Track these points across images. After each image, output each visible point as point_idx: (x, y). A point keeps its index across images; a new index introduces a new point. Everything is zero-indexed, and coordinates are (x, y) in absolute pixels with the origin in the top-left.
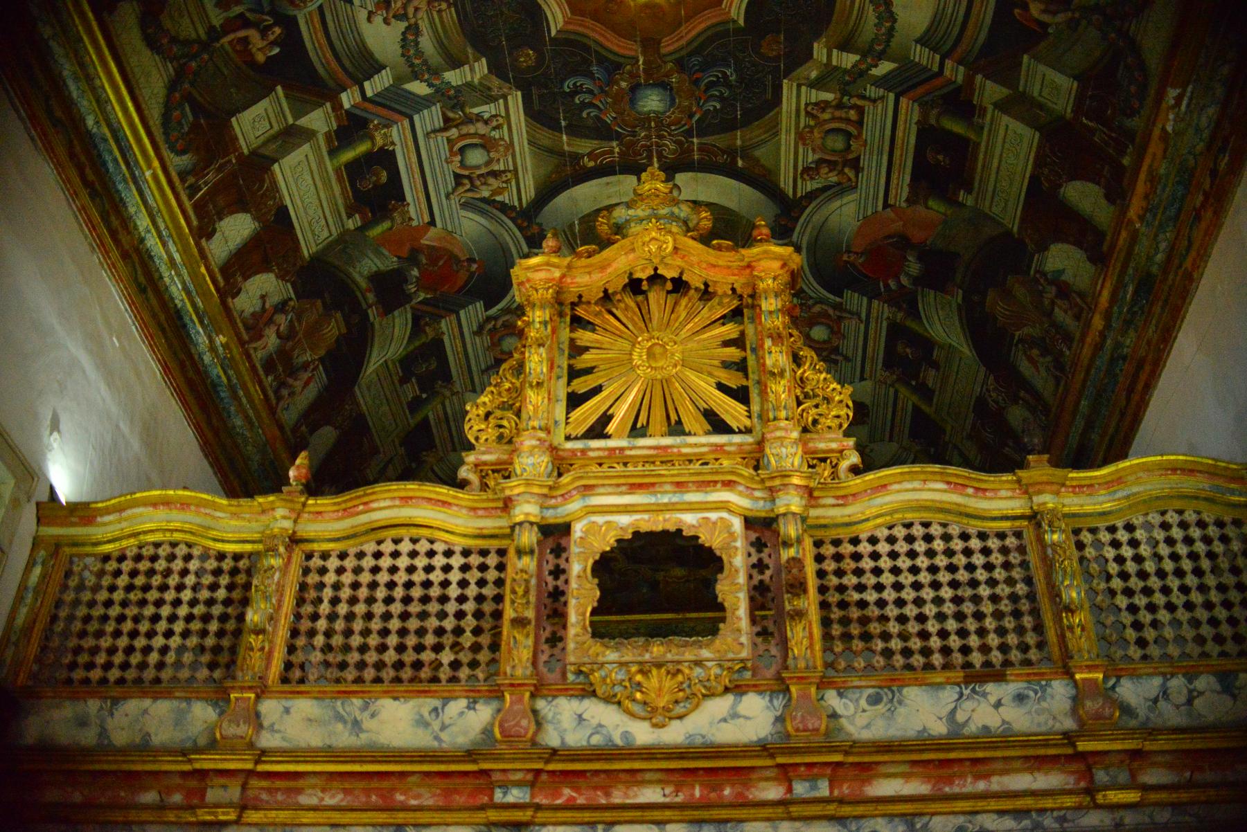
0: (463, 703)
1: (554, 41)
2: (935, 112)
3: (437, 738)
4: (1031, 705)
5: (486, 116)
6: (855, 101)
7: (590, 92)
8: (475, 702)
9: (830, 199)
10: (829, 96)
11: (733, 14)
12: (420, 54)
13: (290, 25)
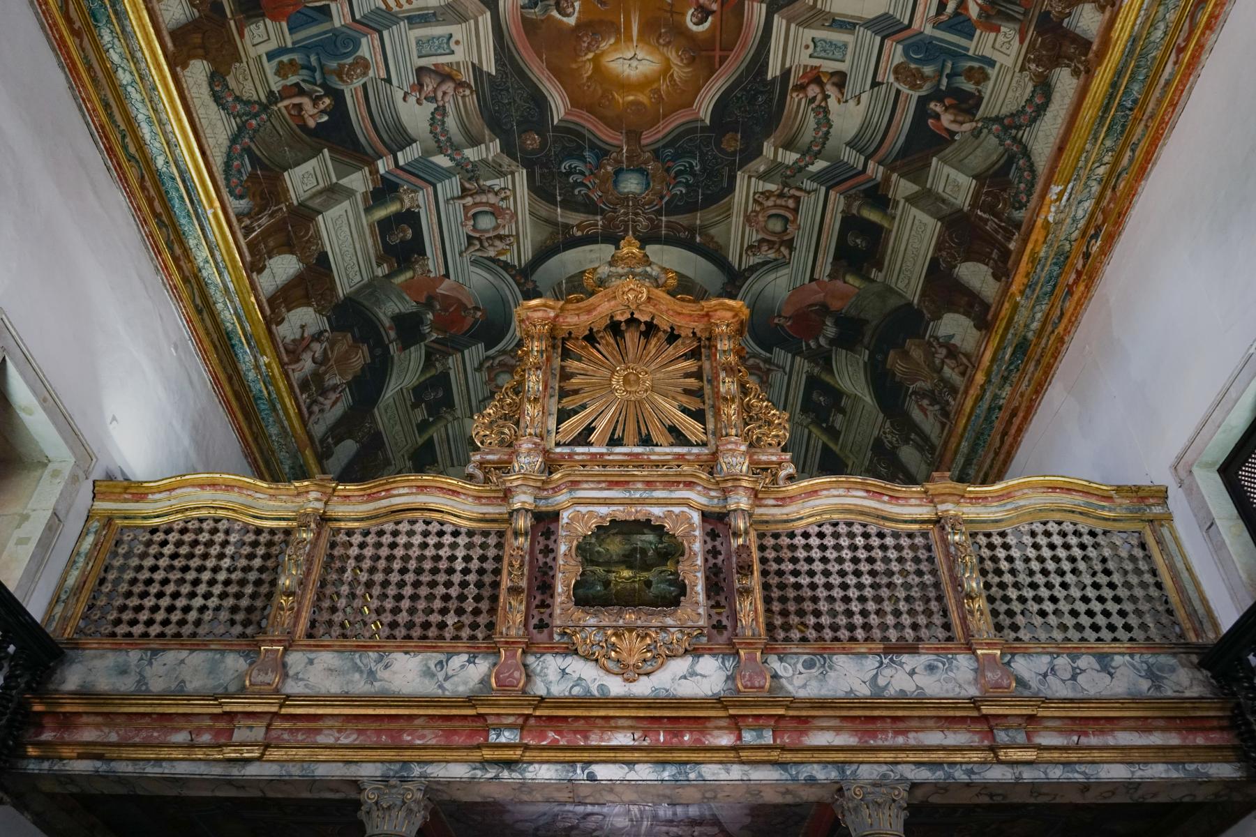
0: (465, 657)
1: (556, 129)
2: (857, 203)
3: (441, 687)
4: (940, 674)
6: (793, 192)
7: (582, 173)
8: (475, 657)
9: (769, 271)
10: (772, 187)
11: (702, 114)
12: (445, 132)
13: (338, 97)
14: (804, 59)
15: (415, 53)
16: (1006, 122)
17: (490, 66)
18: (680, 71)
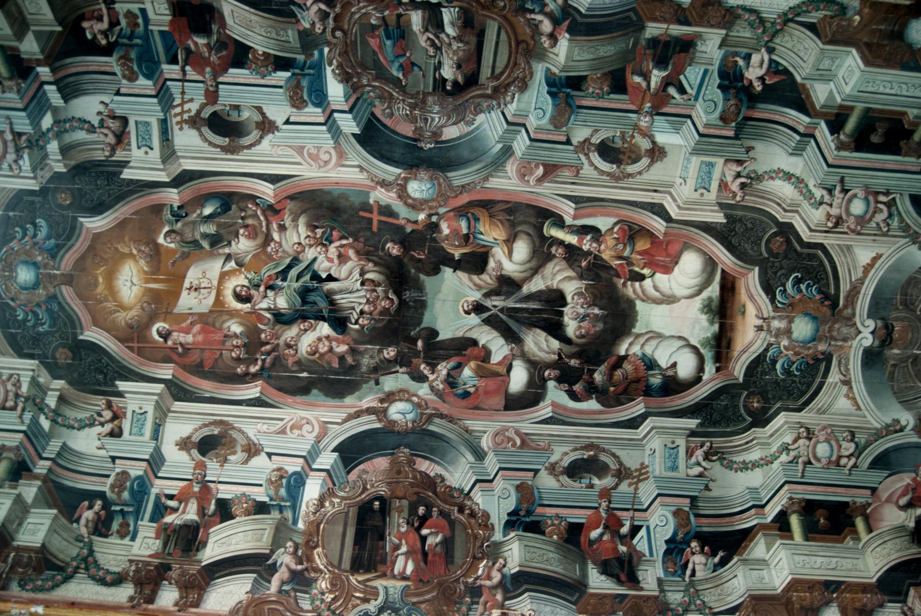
1: (75, 219)
5: (21, 162)
6: (21, 405)
7: (35, 236)
10: (24, 389)
11: (87, 333)
12: (73, 129)
13: (107, 51)
14: (131, 405)
15: (140, 119)
16: (90, 559)
17: (127, 174)
18: (123, 317)
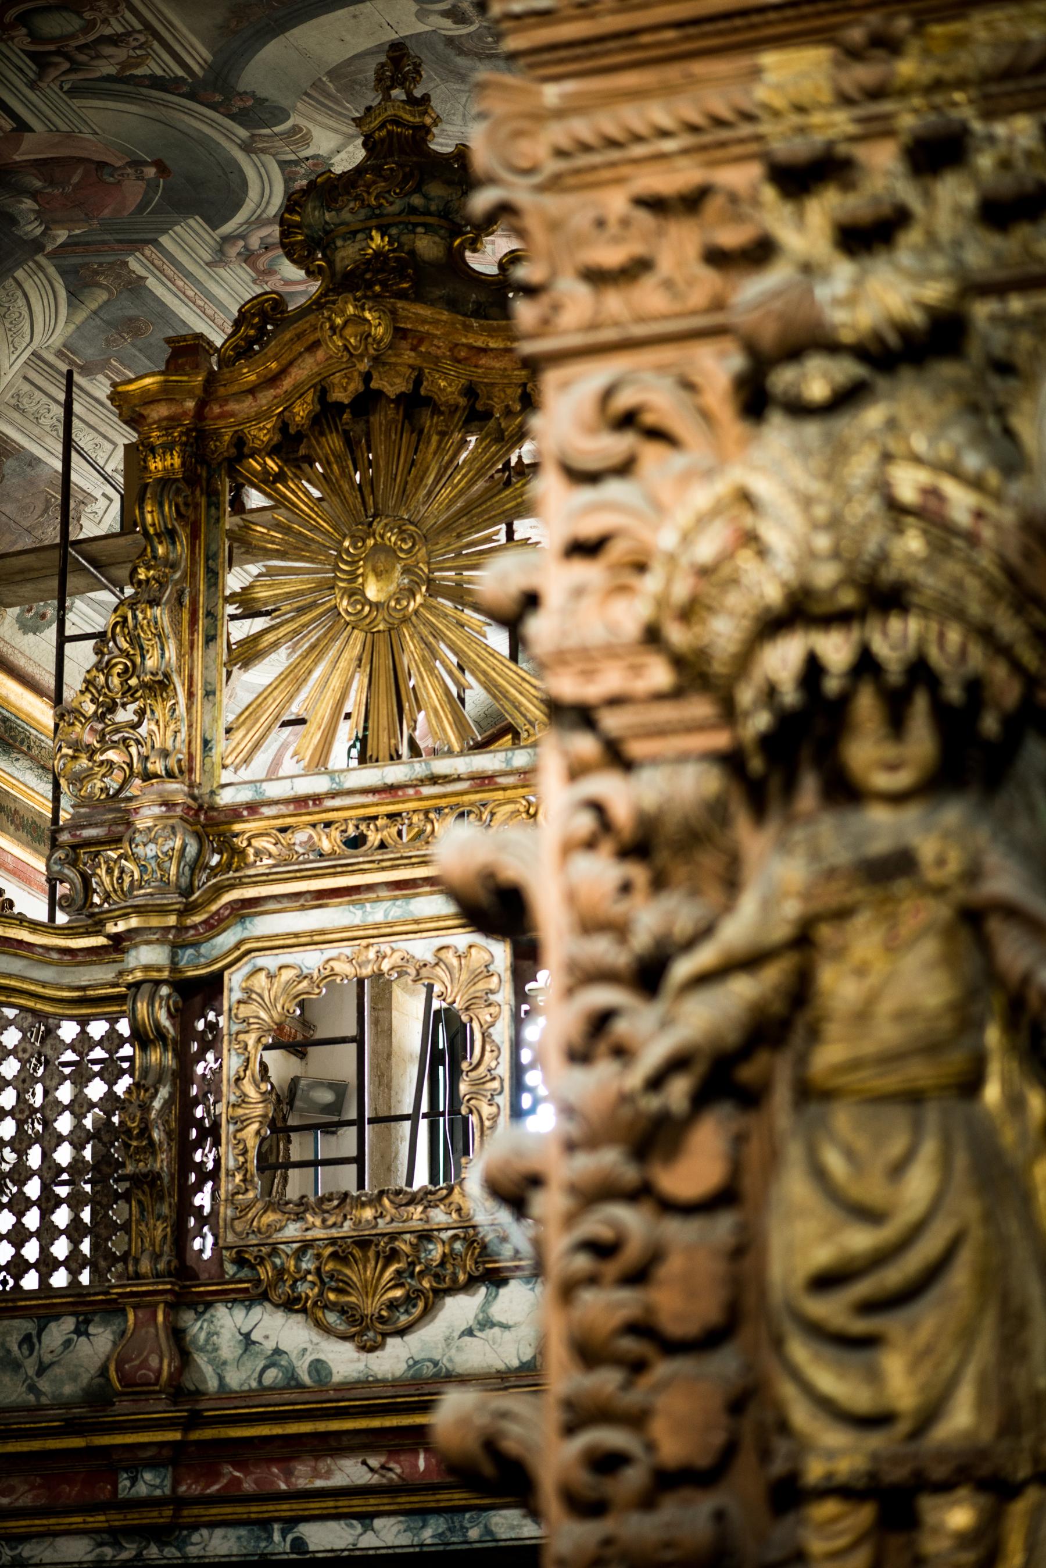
3: (32, 1388)
8: (87, 1322)
